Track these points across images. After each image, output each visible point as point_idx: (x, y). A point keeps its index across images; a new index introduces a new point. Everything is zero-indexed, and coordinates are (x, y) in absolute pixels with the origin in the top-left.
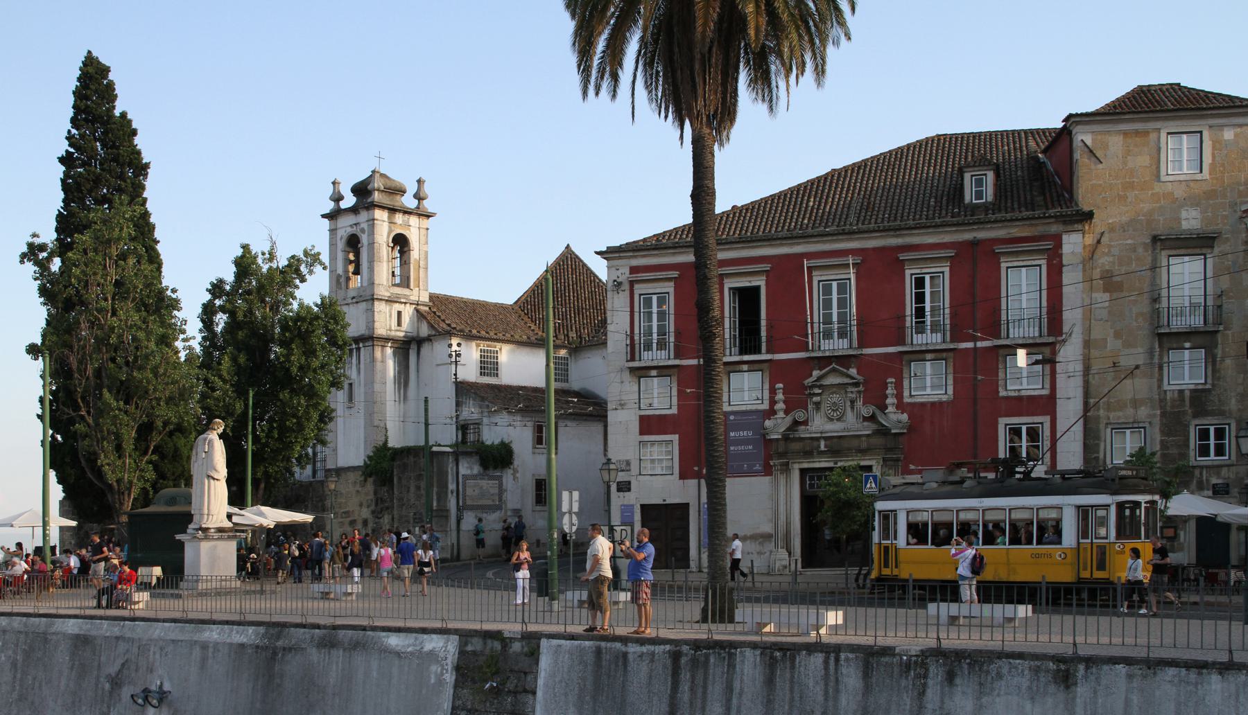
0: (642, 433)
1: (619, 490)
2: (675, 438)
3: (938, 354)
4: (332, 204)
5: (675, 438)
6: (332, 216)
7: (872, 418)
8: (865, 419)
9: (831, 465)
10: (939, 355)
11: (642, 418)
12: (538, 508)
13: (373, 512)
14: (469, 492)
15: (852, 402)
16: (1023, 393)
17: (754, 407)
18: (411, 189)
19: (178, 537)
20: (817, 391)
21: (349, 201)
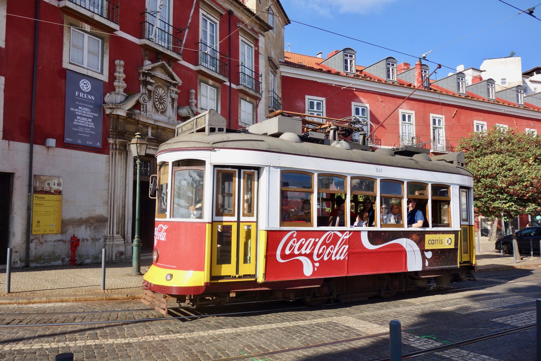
15: (173, 100)
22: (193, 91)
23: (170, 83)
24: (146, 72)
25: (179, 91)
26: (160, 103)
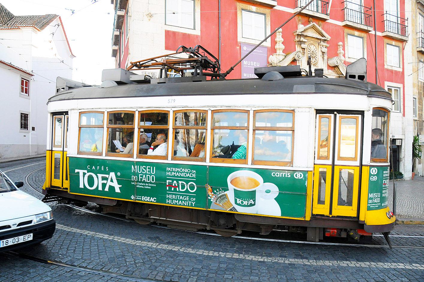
15: (323, 53)
20: (302, 39)
22: (341, 43)
23: (320, 39)
24: (300, 34)
25: (328, 45)
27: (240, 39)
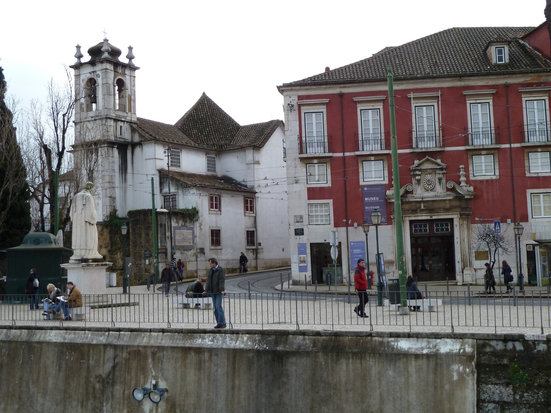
0: (309, 198)
1: (296, 234)
2: (331, 201)
3: (489, 151)
4: (76, 59)
5: (331, 201)
6: (77, 67)
7: (453, 190)
8: (448, 190)
9: (429, 218)
10: (489, 152)
11: (309, 189)
12: (213, 247)
13: (109, 251)
14: (177, 237)
15: (440, 180)
16: (540, 175)
17: (379, 183)
18: (125, 52)
19: (62, 266)
20: (418, 173)
21: (87, 58)
25: (444, 171)
26: (428, 184)
27: (362, 183)
